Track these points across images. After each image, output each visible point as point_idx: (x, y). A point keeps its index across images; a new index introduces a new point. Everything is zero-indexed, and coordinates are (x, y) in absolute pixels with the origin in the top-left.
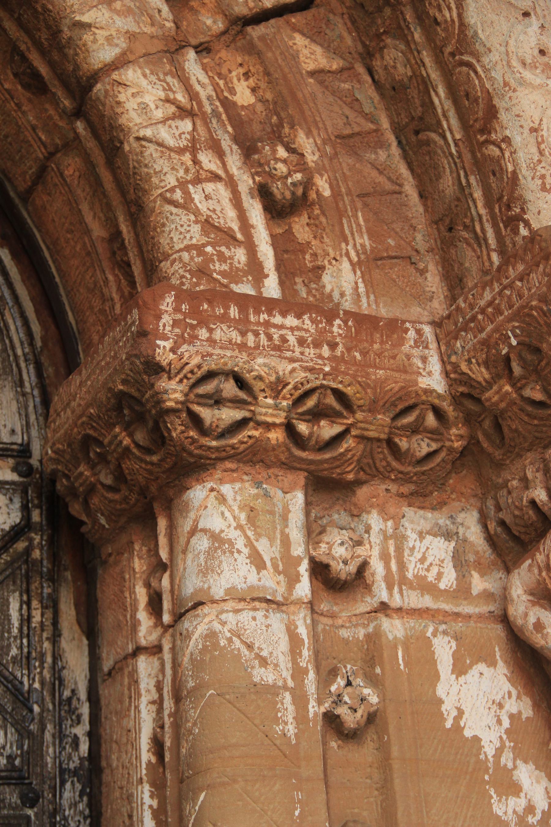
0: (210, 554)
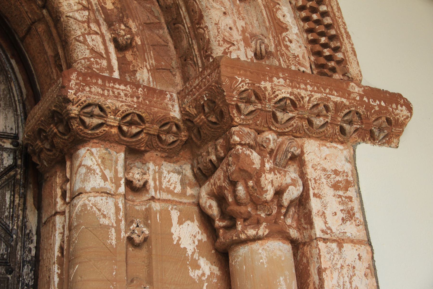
0: (86, 174)
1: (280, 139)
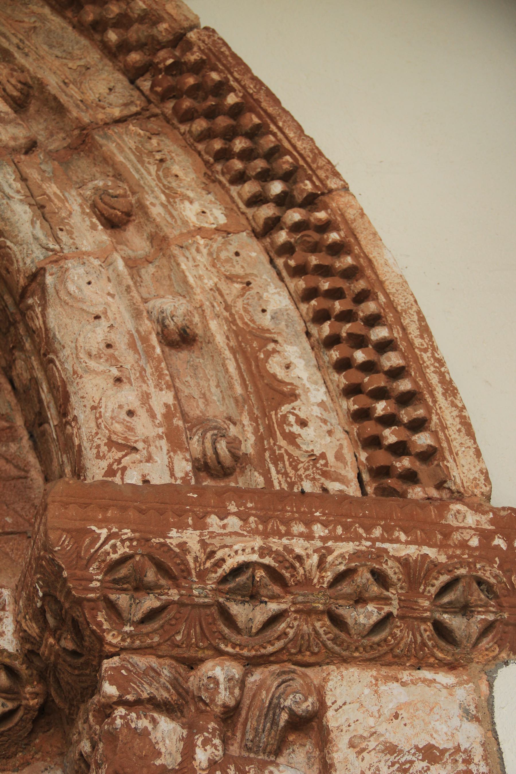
1: (256, 676)
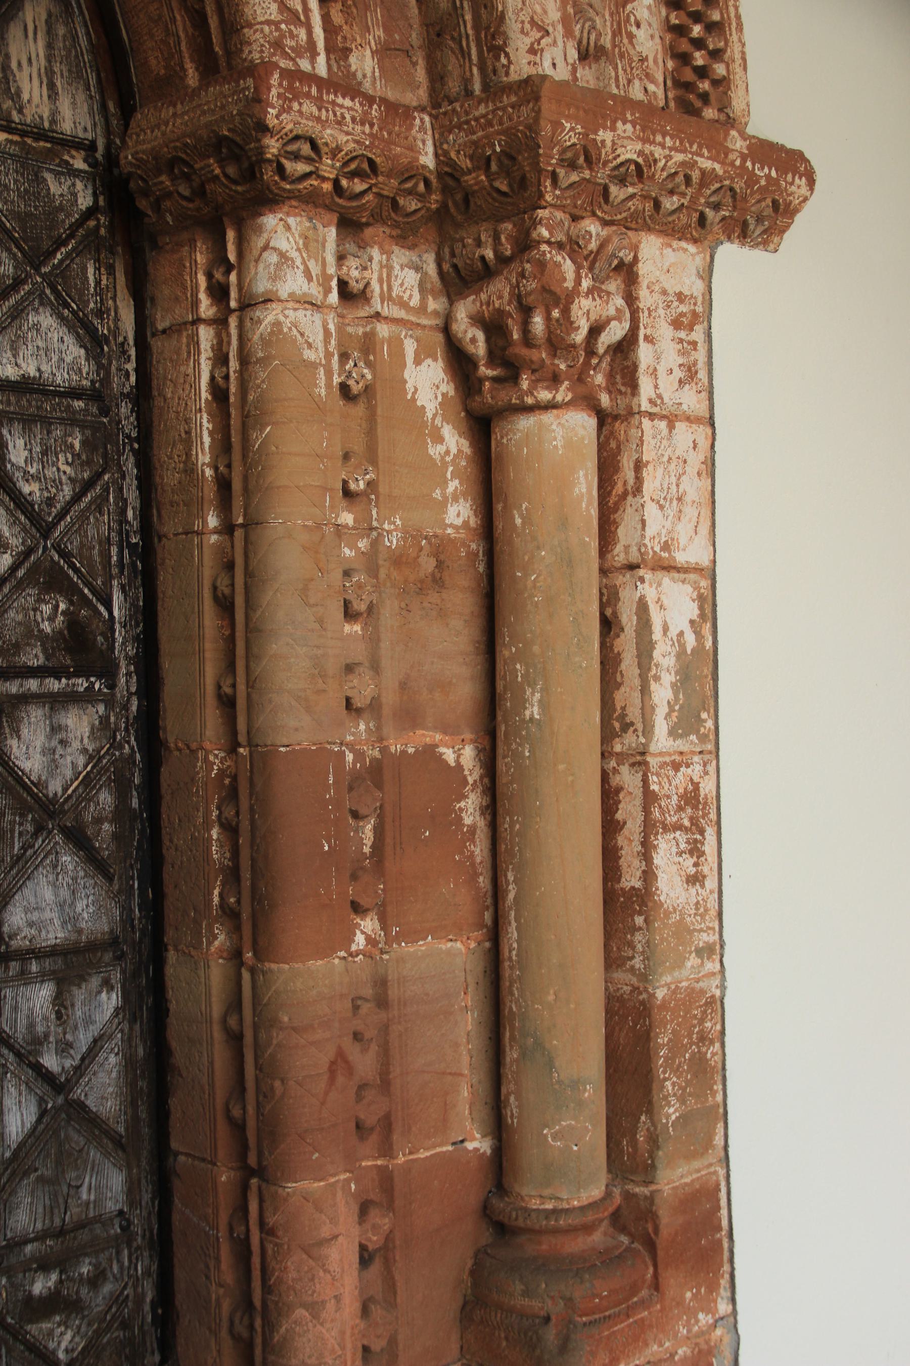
0: (278, 266)
